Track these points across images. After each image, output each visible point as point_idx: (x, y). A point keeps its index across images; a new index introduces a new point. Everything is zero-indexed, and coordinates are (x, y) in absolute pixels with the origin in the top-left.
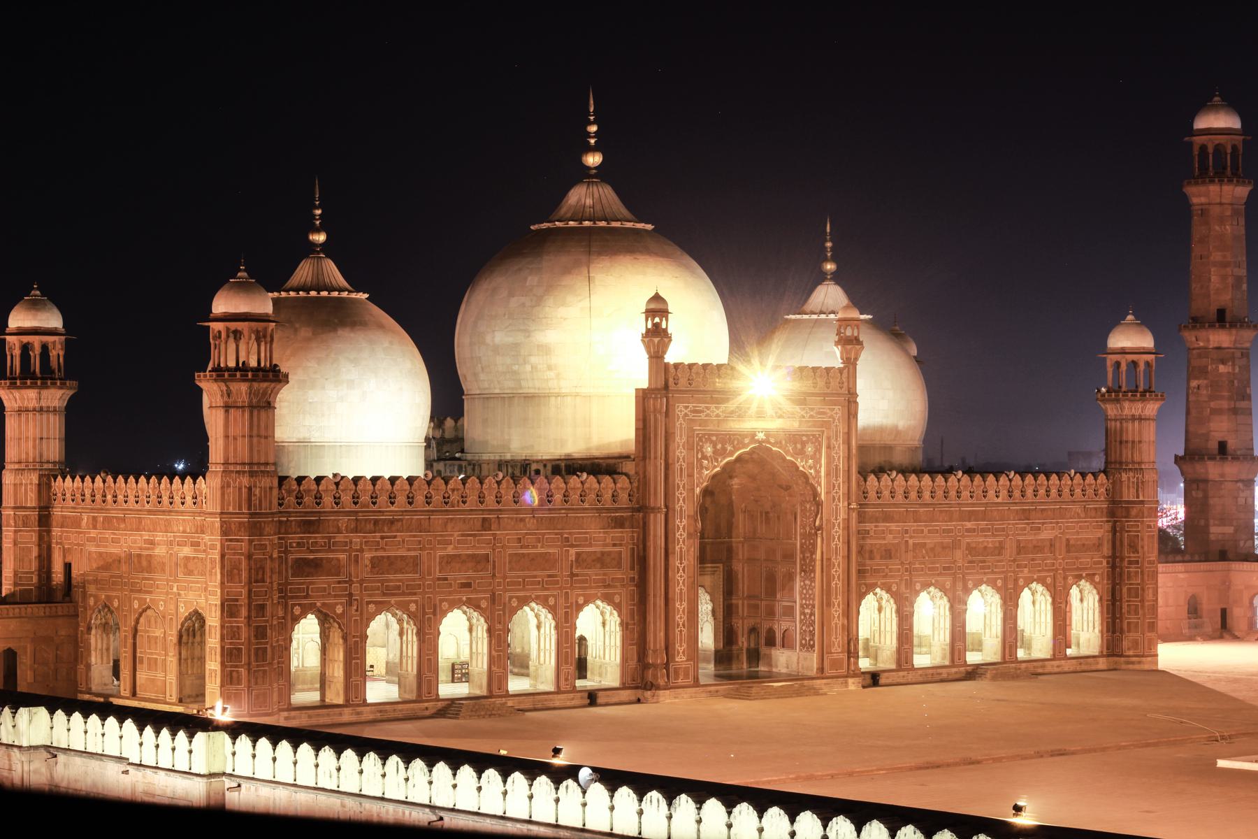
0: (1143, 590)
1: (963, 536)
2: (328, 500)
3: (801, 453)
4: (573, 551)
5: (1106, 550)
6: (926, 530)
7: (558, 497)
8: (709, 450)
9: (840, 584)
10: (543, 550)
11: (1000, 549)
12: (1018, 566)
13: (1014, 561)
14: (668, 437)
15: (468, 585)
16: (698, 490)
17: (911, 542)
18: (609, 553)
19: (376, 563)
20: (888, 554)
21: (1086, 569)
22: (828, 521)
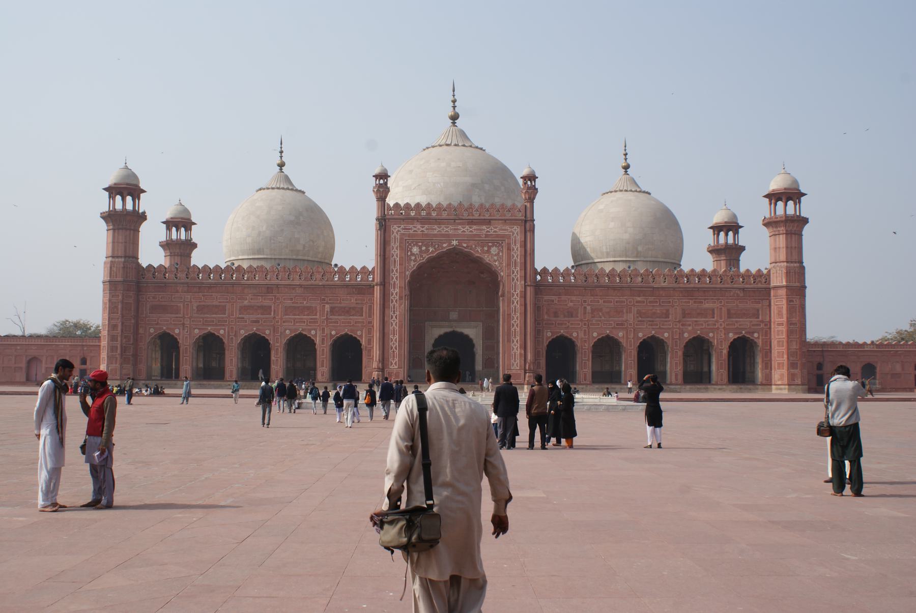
1: (634, 305)
3: (488, 251)
4: (327, 307)
6: (601, 301)
7: (319, 276)
8: (415, 250)
10: (308, 305)
12: (683, 325)
13: (679, 322)
15: (257, 322)
16: (407, 273)
17: (589, 308)
18: (354, 308)
19: (200, 309)
20: (571, 314)
22: (509, 292)
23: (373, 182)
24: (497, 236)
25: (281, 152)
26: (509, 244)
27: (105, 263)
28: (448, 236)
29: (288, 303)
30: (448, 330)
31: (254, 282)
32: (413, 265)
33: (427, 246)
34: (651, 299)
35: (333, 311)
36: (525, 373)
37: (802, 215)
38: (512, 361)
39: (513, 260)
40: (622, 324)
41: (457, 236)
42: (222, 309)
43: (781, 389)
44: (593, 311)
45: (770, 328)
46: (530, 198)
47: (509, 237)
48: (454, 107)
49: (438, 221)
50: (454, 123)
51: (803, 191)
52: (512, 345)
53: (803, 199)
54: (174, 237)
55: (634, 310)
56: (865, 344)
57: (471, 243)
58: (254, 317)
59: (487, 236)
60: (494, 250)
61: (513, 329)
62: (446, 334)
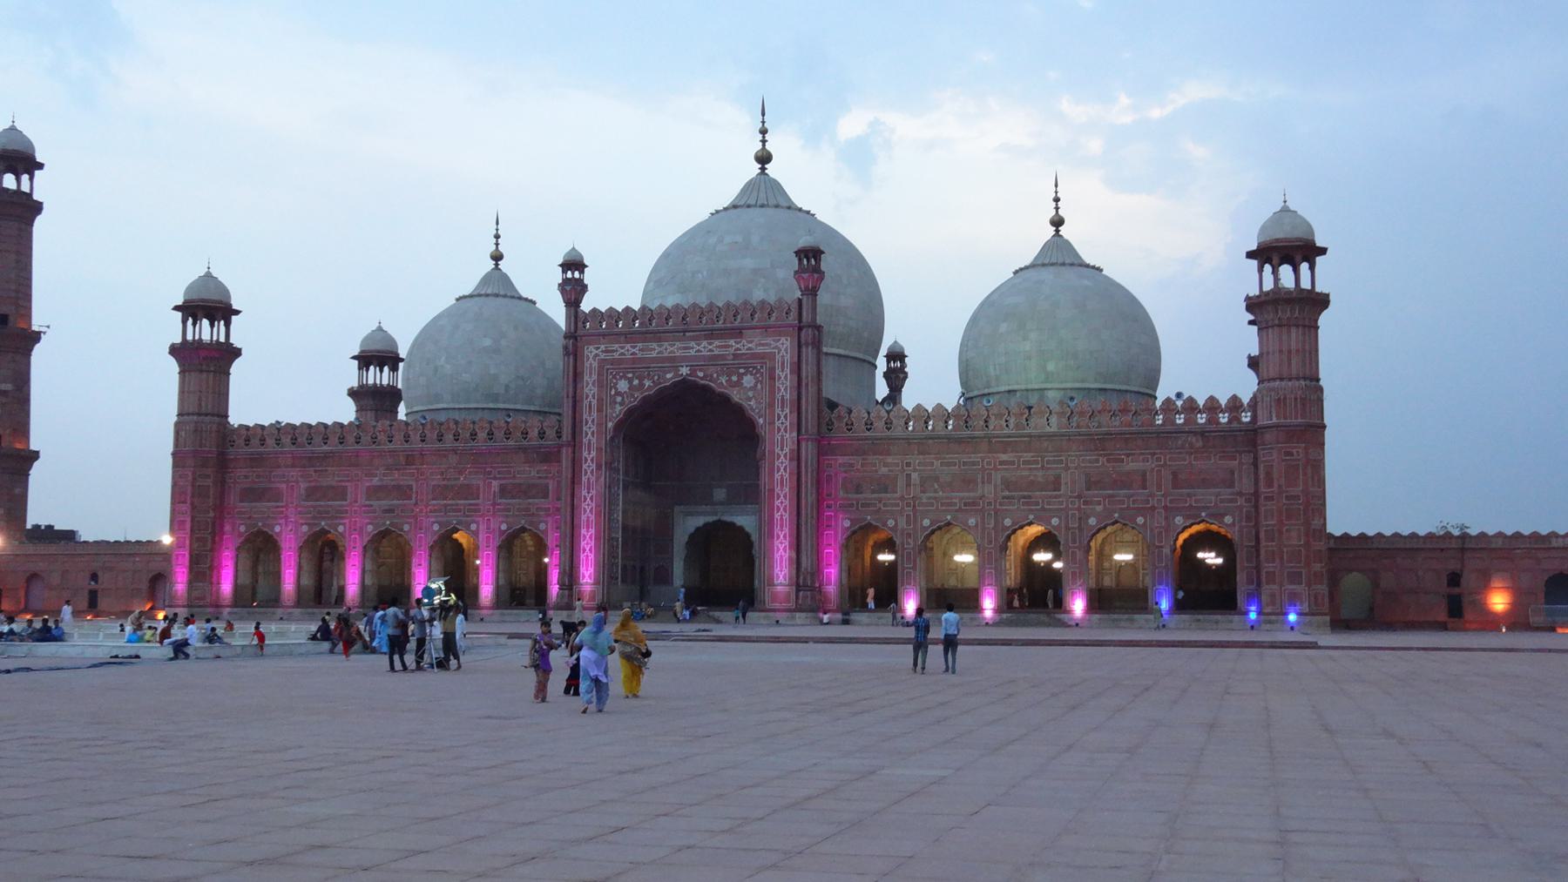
0: (1281, 532)
2: (270, 442)
3: (738, 384)
4: (495, 484)
5: (1246, 485)
6: (937, 463)
7: (482, 435)
8: (623, 386)
9: (786, 516)
11: (1056, 484)
12: (1086, 503)
13: (1079, 497)
14: (577, 376)
15: (390, 511)
16: (610, 425)
17: (915, 476)
19: (312, 493)
20: (884, 486)
21: (1205, 508)
23: (558, 276)
24: (754, 356)
25: (497, 237)
26: (772, 370)
27: (177, 424)
28: (672, 359)
29: (436, 480)
30: (710, 519)
31: (391, 446)
32: (619, 410)
33: (641, 379)
34: (1028, 456)
35: (503, 491)
36: (798, 591)
37: (1318, 289)
38: (777, 571)
39: (778, 396)
40: (974, 504)
41: (685, 358)
42: (341, 493)
43: (1270, 622)
44: (923, 481)
45: (1256, 507)
46: (807, 288)
47: (772, 357)
48: (764, 142)
49: (657, 336)
50: (763, 169)
51: (1318, 244)
52: (776, 543)
53: (1319, 260)
54: (371, 381)
55: (997, 477)
56: (1553, 535)
57: (712, 369)
58: (385, 503)
59: (736, 356)
60: (748, 381)
61: (777, 516)
62: (706, 525)
